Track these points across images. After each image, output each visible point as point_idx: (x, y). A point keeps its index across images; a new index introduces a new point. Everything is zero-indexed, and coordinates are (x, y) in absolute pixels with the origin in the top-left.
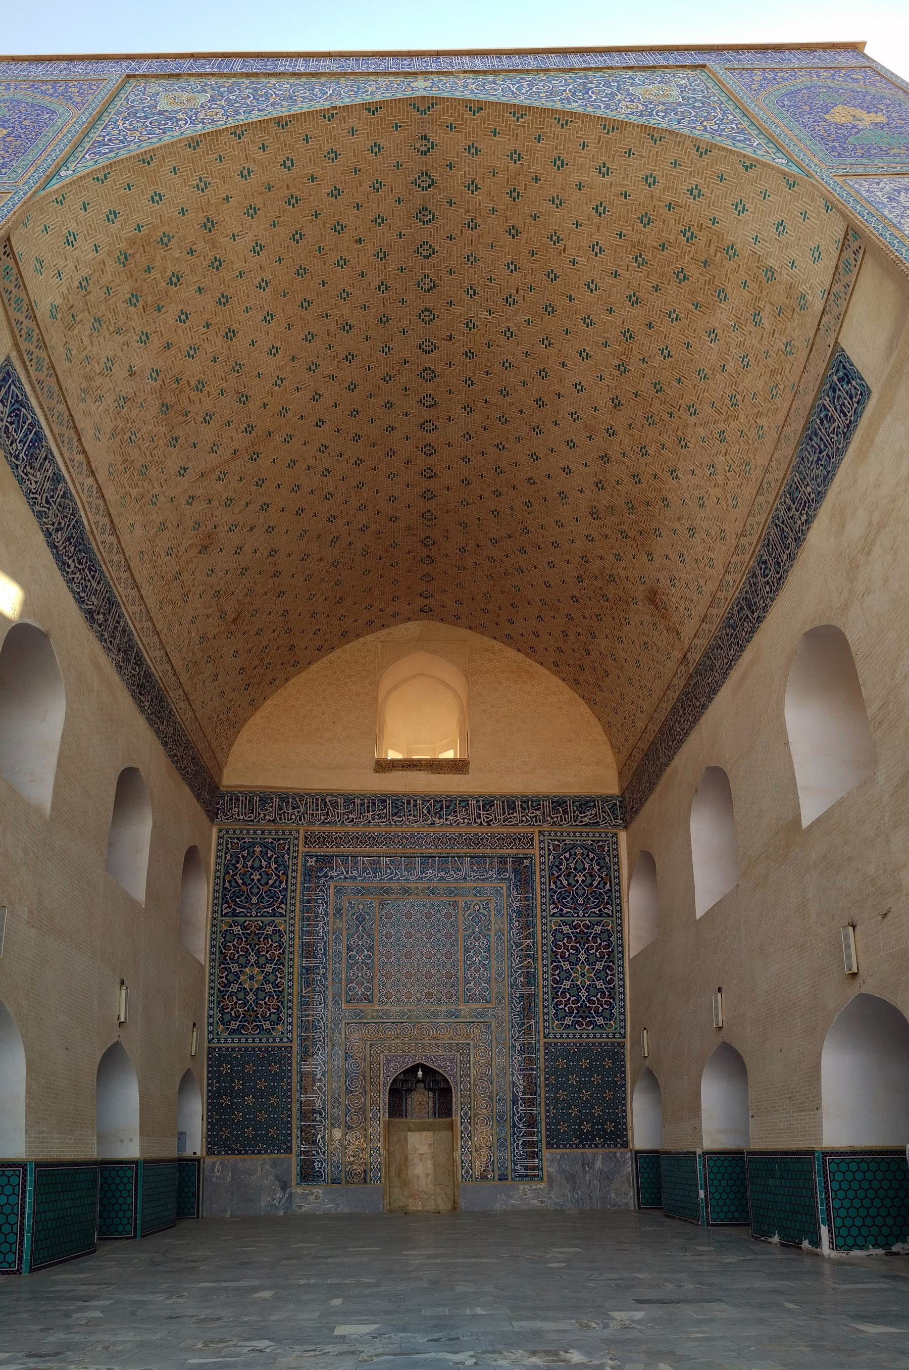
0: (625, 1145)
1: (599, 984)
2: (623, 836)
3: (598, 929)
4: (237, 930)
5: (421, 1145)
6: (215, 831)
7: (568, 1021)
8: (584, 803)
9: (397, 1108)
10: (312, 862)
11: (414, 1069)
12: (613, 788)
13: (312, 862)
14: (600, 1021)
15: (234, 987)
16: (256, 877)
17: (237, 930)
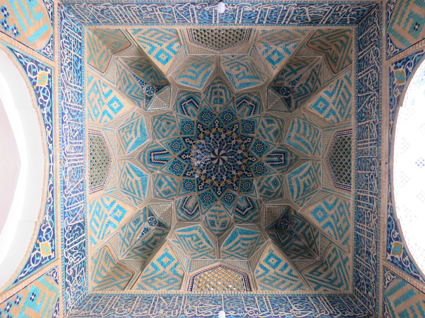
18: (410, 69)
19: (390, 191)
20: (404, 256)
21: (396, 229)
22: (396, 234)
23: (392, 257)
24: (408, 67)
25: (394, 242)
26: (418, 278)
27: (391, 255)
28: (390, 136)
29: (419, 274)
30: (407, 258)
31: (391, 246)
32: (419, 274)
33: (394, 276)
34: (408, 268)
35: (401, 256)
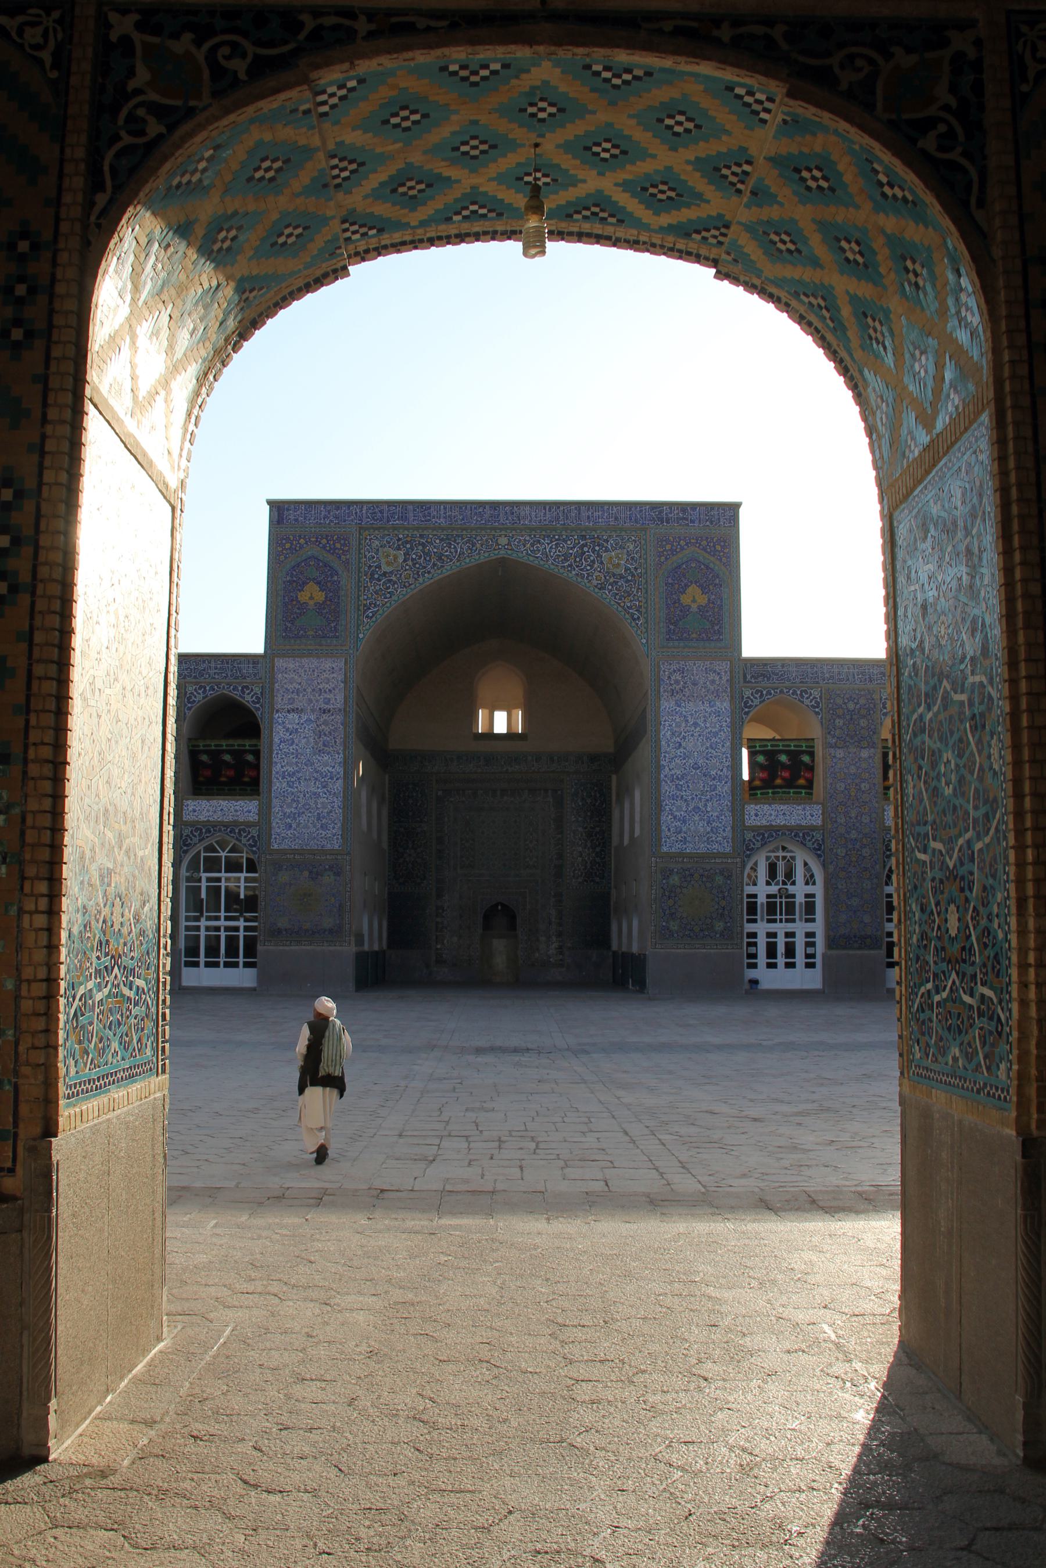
0: (609, 947)
1: (598, 859)
2: (614, 777)
3: (598, 829)
4: (402, 830)
5: (499, 946)
6: (387, 777)
7: (580, 880)
8: (593, 758)
9: (487, 925)
10: (440, 793)
11: (497, 905)
12: (611, 750)
13: (440, 793)
14: (597, 879)
15: (401, 860)
16: (411, 801)
17: (402, 830)
18: (929, 143)
19: (422, 23)
20: (159, 111)
21: (261, 68)
22: (239, 66)
23: (126, 42)
24: (942, 128)
25: (200, 55)
26: (97, 186)
27: (137, 37)
28: (668, 26)
29: (117, 188)
30: (154, 128)
31: (176, 36)
32: (117, 188)
33: (55, 66)
34: (117, 138)
35: (153, 96)
